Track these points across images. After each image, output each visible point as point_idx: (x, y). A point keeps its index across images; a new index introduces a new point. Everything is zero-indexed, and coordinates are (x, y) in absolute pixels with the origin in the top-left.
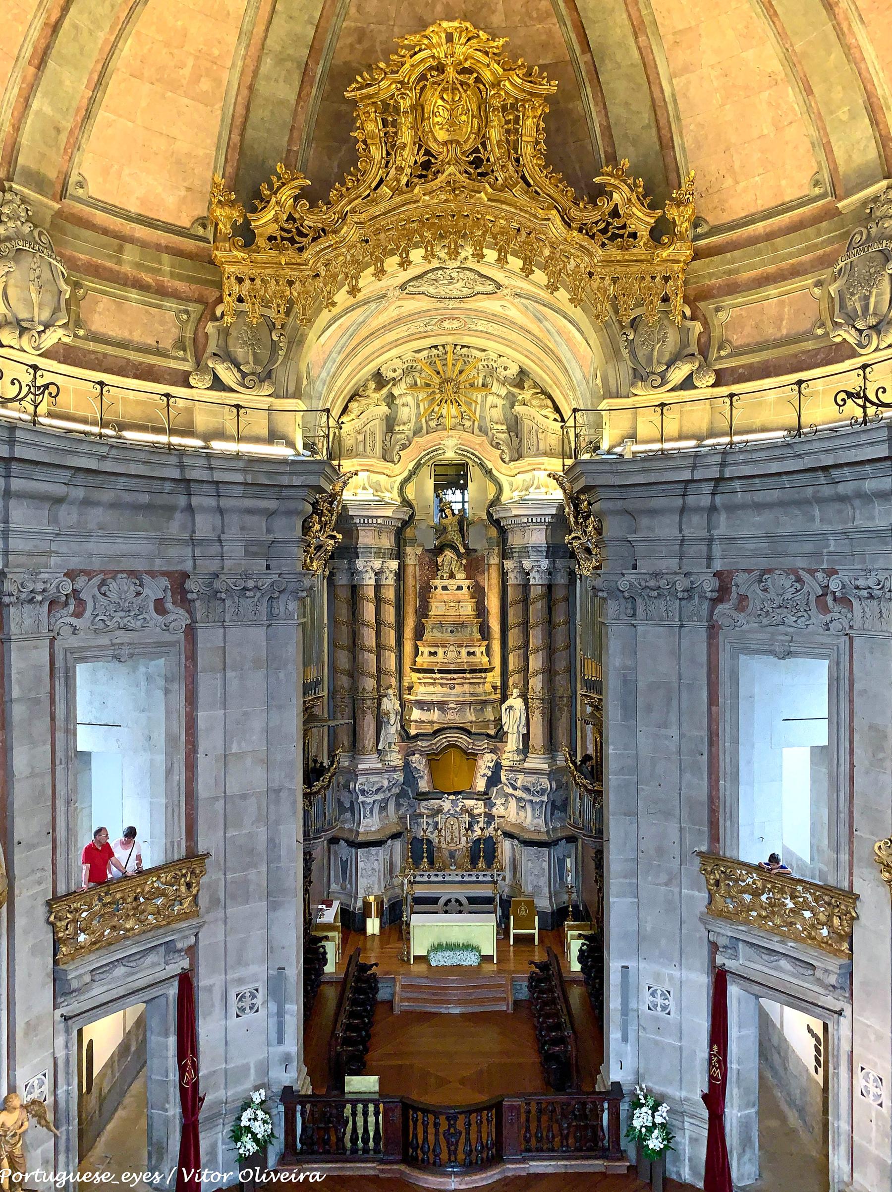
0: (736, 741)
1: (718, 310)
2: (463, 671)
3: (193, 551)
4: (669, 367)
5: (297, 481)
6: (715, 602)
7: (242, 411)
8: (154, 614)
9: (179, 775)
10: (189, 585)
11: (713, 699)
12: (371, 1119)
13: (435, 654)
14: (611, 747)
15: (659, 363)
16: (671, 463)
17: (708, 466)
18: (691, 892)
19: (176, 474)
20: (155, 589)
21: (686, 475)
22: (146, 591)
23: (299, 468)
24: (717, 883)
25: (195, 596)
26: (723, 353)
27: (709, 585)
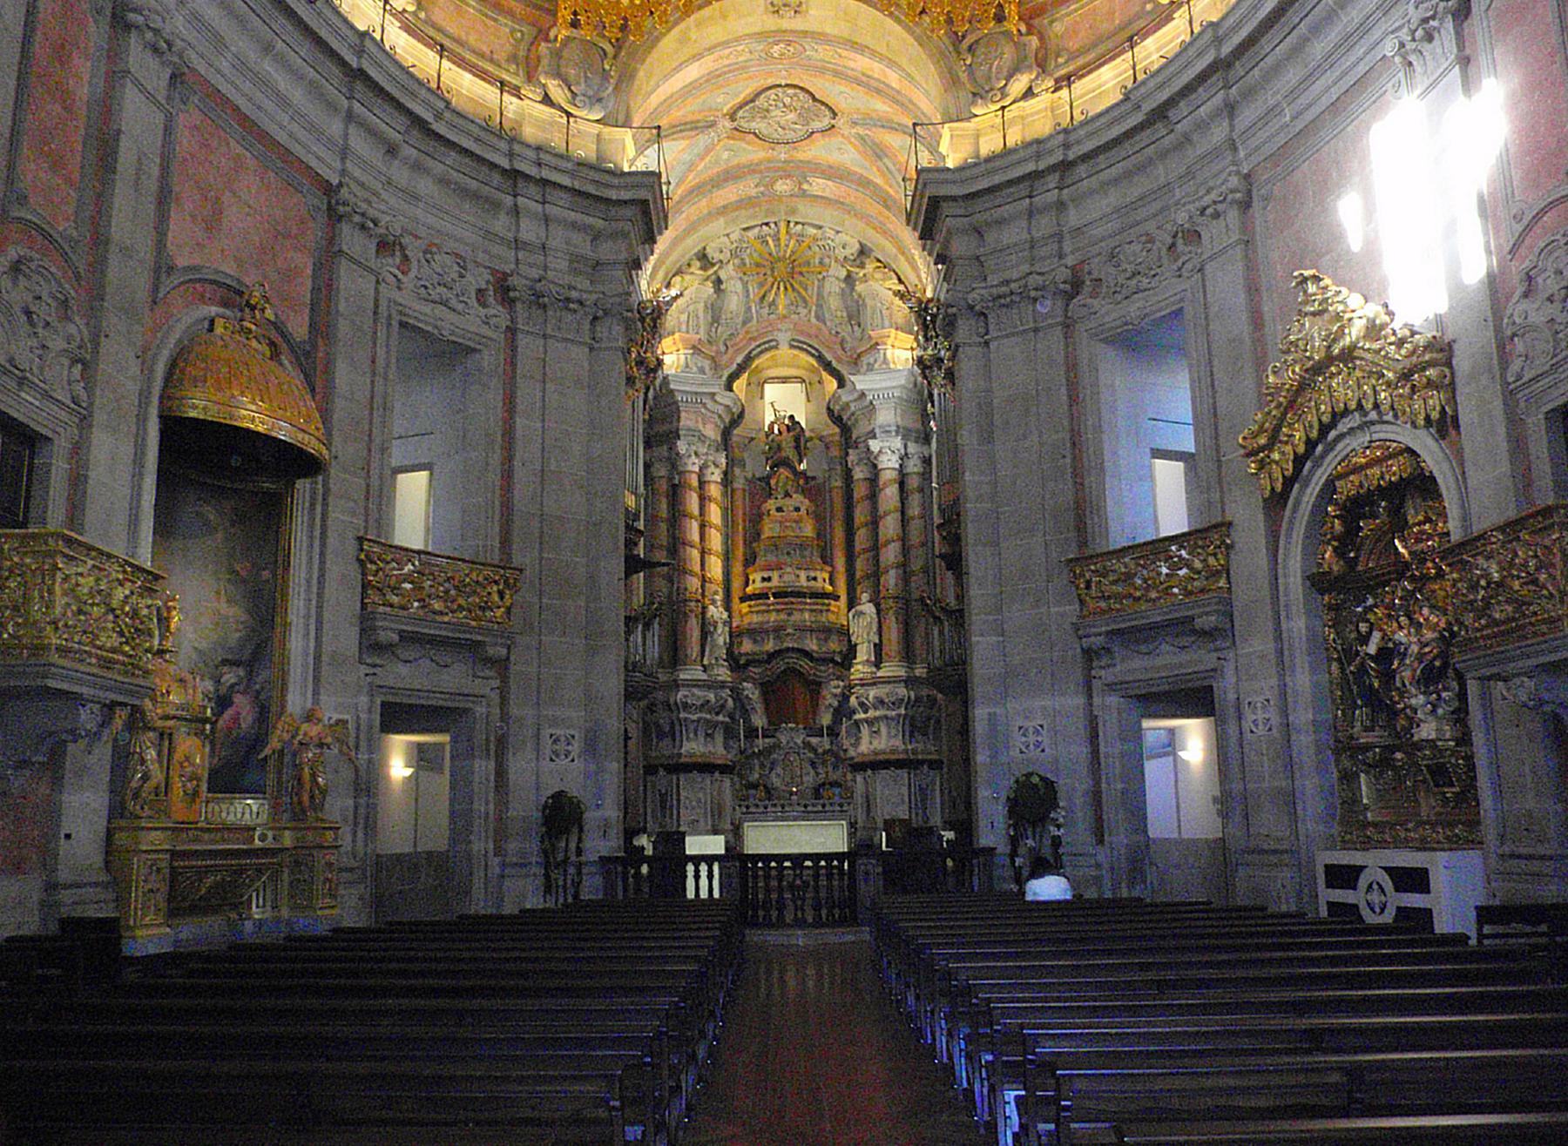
0: (1098, 428)
1: (1052, 22)
2: (803, 595)
3: (516, 254)
4: (1008, 81)
5: (626, 195)
6: (1069, 296)
7: (572, 120)
8: (476, 305)
9: (494, 478)
10: (514, 281)
11: (1073, 399)
12: (704, 882)
13: (769, 579)
14: (967, 474)
15: (998, 79)
16: (1015, 157)
17: (1051, 152)
18: (1062, 609)
19: (505, 163)
20: (478, 279)
21: (1030, 167)
22: (469, 277)
23: (629, 180)
24: (1088, 587)
25: (517, 294)
26: (1061, 60)
27: (1063, 274)
